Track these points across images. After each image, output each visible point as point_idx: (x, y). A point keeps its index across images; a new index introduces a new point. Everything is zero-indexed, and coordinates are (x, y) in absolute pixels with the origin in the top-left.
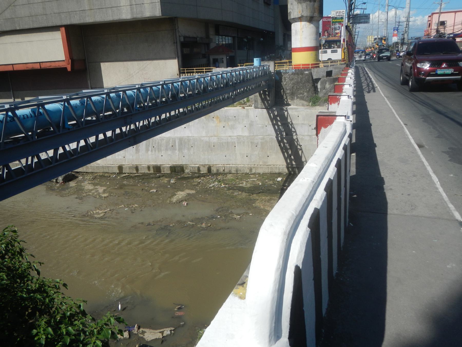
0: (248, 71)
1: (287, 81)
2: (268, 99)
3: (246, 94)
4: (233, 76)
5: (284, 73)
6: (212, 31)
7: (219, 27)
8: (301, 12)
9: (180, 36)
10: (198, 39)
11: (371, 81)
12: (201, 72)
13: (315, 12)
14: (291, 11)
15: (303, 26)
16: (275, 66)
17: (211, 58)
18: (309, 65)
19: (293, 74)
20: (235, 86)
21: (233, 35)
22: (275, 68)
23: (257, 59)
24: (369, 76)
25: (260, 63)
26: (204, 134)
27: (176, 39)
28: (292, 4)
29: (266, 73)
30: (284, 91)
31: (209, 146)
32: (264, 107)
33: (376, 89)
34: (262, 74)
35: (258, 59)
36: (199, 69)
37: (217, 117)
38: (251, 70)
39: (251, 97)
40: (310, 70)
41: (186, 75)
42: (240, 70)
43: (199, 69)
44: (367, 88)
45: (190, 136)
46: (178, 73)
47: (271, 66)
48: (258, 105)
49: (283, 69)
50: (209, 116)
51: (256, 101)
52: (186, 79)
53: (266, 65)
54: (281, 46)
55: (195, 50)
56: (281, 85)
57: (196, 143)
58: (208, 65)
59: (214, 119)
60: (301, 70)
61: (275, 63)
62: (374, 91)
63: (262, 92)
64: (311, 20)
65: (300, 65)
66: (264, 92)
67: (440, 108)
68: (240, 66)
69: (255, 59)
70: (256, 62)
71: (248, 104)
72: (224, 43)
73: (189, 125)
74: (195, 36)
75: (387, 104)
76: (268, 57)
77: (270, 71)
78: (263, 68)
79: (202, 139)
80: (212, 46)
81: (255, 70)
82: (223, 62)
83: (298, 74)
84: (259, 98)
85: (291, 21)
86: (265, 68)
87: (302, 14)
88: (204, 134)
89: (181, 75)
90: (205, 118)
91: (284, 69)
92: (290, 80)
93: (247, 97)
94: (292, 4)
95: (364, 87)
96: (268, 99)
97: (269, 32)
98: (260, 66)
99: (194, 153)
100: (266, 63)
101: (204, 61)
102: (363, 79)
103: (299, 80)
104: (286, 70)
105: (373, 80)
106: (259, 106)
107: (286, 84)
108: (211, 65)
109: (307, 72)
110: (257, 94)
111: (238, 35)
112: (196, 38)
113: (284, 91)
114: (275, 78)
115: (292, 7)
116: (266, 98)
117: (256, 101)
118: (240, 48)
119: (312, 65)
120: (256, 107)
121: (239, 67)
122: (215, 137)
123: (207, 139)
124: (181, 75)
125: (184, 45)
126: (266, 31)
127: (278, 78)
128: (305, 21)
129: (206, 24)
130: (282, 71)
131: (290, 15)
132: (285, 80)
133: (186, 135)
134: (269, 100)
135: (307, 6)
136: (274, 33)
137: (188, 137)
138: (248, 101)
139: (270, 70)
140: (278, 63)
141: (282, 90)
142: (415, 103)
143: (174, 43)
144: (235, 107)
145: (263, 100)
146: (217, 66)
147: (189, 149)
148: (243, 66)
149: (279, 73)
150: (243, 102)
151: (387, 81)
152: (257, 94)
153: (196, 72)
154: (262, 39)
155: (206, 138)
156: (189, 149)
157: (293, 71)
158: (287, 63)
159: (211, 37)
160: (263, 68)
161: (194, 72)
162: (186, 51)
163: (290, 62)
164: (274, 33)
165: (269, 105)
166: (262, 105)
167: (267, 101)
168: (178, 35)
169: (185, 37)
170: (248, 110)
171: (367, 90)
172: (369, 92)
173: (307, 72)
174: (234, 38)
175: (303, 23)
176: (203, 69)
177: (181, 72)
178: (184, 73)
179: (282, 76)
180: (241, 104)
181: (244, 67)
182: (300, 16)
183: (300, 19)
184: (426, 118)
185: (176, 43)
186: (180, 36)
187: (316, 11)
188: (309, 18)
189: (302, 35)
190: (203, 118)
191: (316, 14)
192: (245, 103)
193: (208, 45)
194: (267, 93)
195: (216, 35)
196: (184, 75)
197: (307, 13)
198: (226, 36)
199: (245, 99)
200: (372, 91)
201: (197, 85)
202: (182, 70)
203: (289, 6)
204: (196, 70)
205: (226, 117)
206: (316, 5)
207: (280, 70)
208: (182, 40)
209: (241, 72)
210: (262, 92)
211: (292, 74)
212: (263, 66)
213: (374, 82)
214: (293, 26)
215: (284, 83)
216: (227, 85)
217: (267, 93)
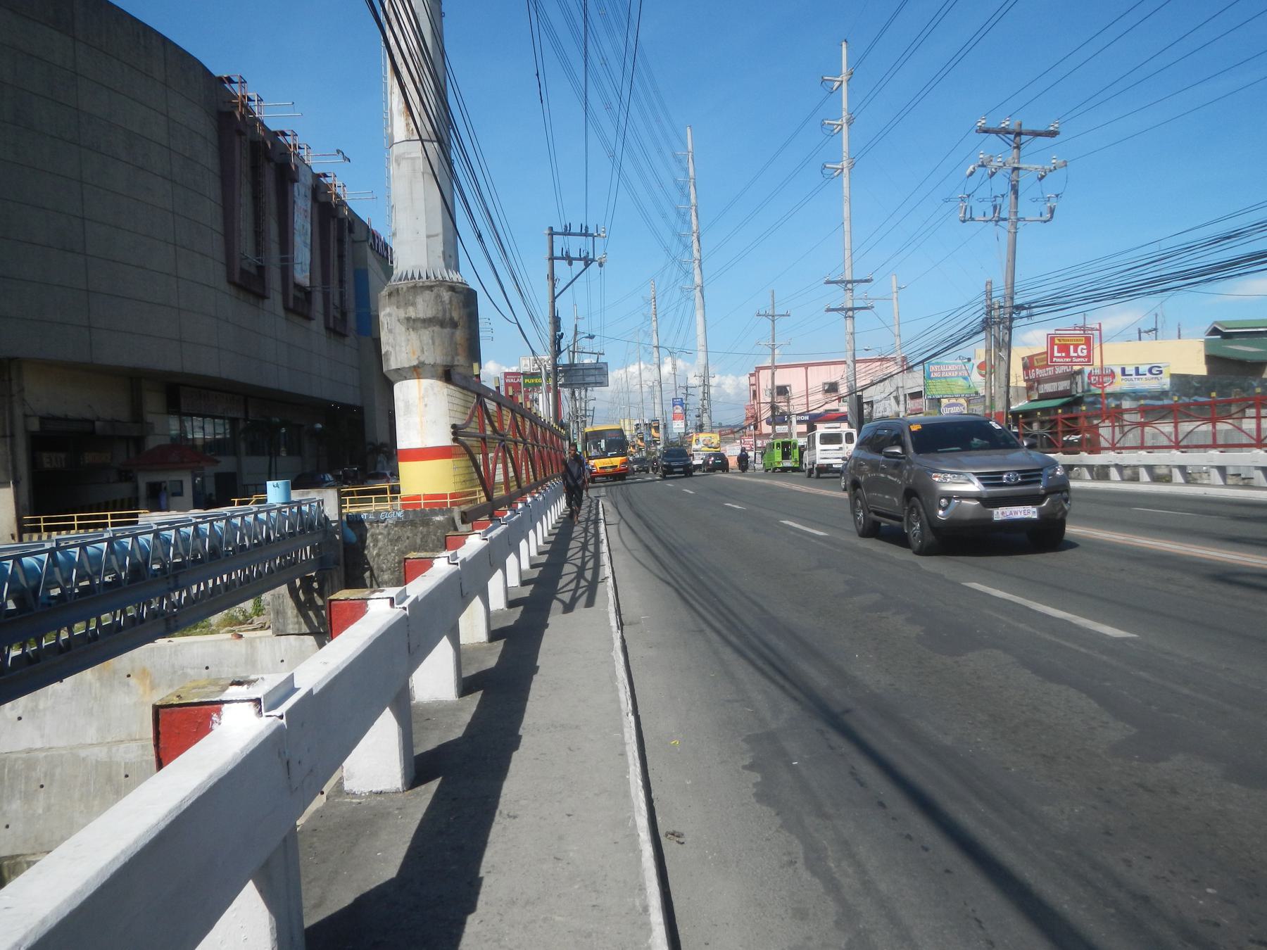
0: (238, 521)
1: (380, 544)
2: (320, 602)
3: (252, 587)
4: (168, 541)
5: (371, 523)
6: (153, 403)
7: (181, 392)
8: (418, 353)
9: (26, 416)
10: (97, 423)
11: (597, 555)
12: (96, 526)
13: (457, 354)
14: (391, 349)
15: (426, 390)
16: (341, 503)
17: (143, 481)
18: (444, 496)
19: (399, 523)
20: (175, 575)
21: (231, 415)
22: (340, 508)
23: (275, 482)
24: (597, 534)
25: (288, 495)
26: (91, 735)
27: (12, 422)
28: (390, 331)
29: (313, 527)
30: (372, 575)
31: (109, 779)
32: (305, 629)
33: (600, 586)
34: (292, 526)
35: (279, 482)
36: (121, 516)
37: (144, 673)
38: (250, 519)
39: (267, 597)
40: (450, 510)
41: (45, 536)
42: (237, 513)
43: (121, 516)
44: (572, 586)
45: (38, 745)
46: (15, 531)
47: (327, 502)
48: (285, 624)
49: (367, 510)
50: (115, 672)
51: (279, 613)
52: (72, 543)
53: (310, 503)
54: (383, 445)
55: (89, 458)
56: (365, 556)
57: (58, 771)
58: (133, 503)
59: (132, 681)
60: (423, 511)
61: (340, 495)
62: (590, 603)
63: (298, 582)
64: (447, 376)
65: (417, 497)
66: (307, 582)
67: (818, 678)
68: (240, 503)
69: (270, 484)
70: (275, 492)
71: (257, 621)
72: (199, 435)
73: (34, 711)
74: (88, 415)
75: (613, 677)
76: (337, 478)
77: (326, 518)
78: (299, 508)
79: (83, 753)
80: (152, 443)
81: (274, 514)
82: (180, 494)
83: (413, 523)
84: (289, 603)
85: (391, 378)
86: (305, 508)
87: (422, 359)
88: (91, 735)
89: (26, 536)
90: (100, 679)
91: (373, 509)
92: (391, 541)
93: (256, 594)
94: (390, 331)
95: (561, 583)
96: (320, 602)
97: (347, 408)
98: (289, 503)
99: (48, 808)
100: (313, 494)
101: (124, 490)
102: (574, 545)
103: (418, 541)
104: (377, 513)
105: (604, 548)
106: (291, 628)
107: (378, 555)
108: (142, 502)
109: (439, 518)
110: (284, 589)
111: (246, 413)
112: (93, 422)
113: (372, 575)
114: (343, 537)
115: (391, 340)
116: (311, 601)
117: (279, 613)
118: (254, 450)
119: (453, 496)
120: (280, 633)
121: (236, 507)
122: (134, 745)
123: (101, 753)
124: (26, 536)
125: (40, 442)
126: (337, 404)
127: (352, 536)
128: (432, 377)
129: (135, 381)
130: (364, 516)
131: (388, 360)
132: (376, 541)
133: (24, 745)
134: (323, 607)
135: (433, 338)
136: (361, 410)
137: (30, 751)
138: (259, 611)
139: (327, 512)
140: (351, 493)
141: (367, 574)
142: (728, 654)
143: (4, 436)
144: (212, 633)
145: (302, 608)
146: (163, 502)
147: (28, 797)
148: (247, 503)
149: (356, 523)
150: (241, 618)
151: (648, 548)
152: (284, 589)
153: (113, 524)
154: (319, 426)
155: (96, 750)
156: (28, 797)
157: (399, 515)
158: (384, 491)
159: (149, 418)
160: (299, 508)
161: (72, 527)
162: (50, 460)
163: (396, 490)
164: (361, 410)
165: (322, 624)
166: (298, 623)
167: (317, 610)
168: (18, 412)
169: (44, 420)
170: (251, 642)
171: (566, 597)
172: (568, 608)
173: (439, 518)
174: (233, 422)
175: (426, 382)
176: (72, 519)
177: (23, 529)
178: (37, 530)
179: (366, 530)
180: (232, 622)
181: (225, 510)
182: (415, 363)
183: (416, 371)
184: (766, 754)
185: (12, 436)
186: (26, 416)
187: (460, 350)
188: (440, 370)
189: (422, 414)
190: (88, 675)
191: (461, 360)
192: (247, 619)
193: (139, 441)
194: (315, 585)
195: (169, 413)
196: (35, 537)
197: (435, 356)
198: (204, 416)
199: (248, 605)
200: (583, 600)
201: (108, 560)
202: (31, 521)
203: (384, 336)
204: (79, 518)
205: (175, 672)
206: (460, 335)
207: (358, 515)
208: (35, 425)
209: (206, 527)
210: (298, 582)
211: (396, 525)
212: (299, 503)
213: (605, 558)
214: (398, 388)
215: (371, 552)
216: (139, 571)
217: (315, 585)
